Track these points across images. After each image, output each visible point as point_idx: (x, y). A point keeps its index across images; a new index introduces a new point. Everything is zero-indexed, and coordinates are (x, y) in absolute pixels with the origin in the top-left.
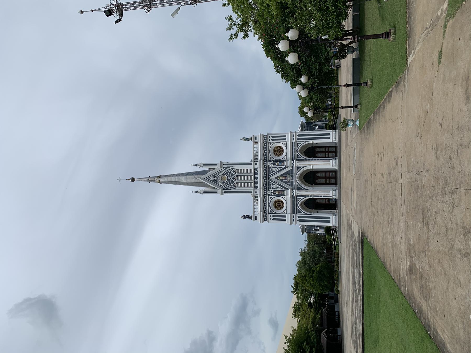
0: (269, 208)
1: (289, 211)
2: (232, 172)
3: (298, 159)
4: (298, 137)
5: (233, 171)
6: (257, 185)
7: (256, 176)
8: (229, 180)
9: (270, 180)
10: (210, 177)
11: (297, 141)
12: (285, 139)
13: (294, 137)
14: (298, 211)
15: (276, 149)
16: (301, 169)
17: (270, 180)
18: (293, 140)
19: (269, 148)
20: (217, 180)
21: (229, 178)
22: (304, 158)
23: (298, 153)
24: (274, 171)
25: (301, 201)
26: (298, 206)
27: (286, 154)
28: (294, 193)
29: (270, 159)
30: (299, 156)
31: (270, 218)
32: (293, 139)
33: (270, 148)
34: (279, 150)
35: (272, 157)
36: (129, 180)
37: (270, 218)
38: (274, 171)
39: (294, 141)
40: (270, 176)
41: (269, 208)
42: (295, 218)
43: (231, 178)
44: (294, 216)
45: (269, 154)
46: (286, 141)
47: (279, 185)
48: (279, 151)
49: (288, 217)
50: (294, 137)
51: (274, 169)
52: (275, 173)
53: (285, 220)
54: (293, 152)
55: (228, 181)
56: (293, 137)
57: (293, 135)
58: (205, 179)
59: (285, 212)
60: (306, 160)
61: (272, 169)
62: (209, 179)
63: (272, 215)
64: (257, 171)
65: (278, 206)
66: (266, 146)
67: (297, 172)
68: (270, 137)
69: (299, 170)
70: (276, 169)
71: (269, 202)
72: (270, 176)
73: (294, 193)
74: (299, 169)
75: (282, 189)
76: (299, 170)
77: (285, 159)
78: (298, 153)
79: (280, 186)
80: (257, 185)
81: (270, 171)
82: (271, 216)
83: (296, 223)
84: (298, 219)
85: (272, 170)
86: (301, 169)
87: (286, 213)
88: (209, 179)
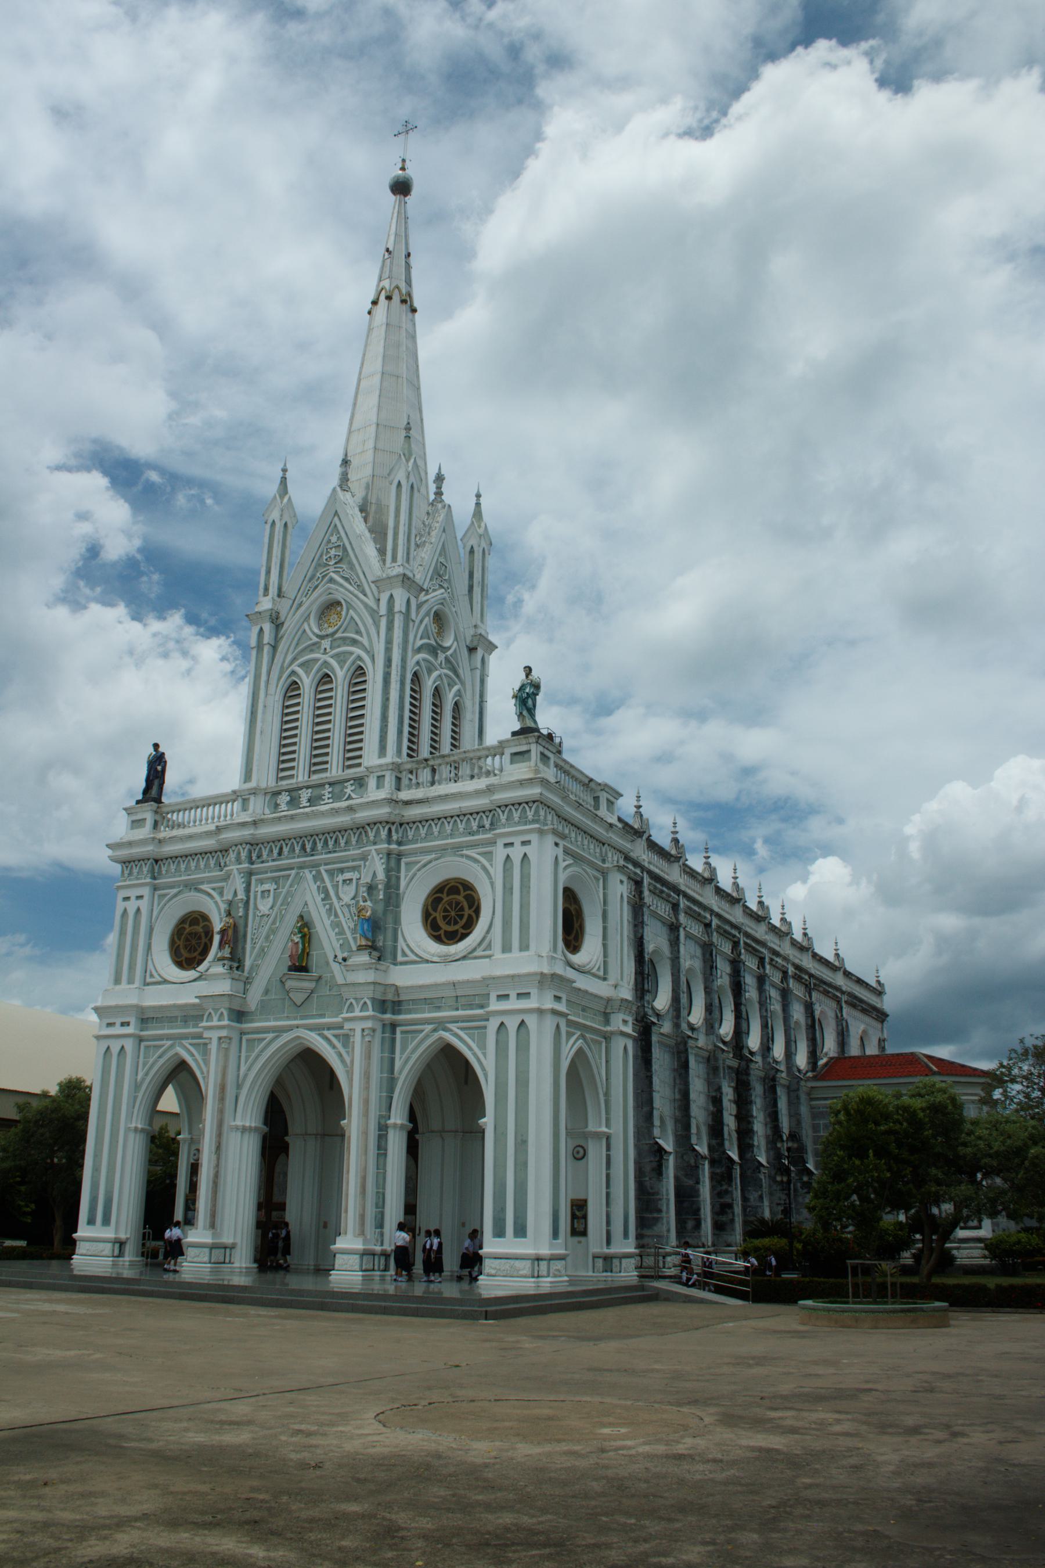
0: (175, 891)
1: (156, 998)
2: (357, 651)
3: (398, 1036)
4: (512, 1024)
5: (359, 658)
6: (283, 807)
7: (327, 795)
8: (313, 647)
9: (299, 879)
10: (339, 538)
11: (493, 1025)
12: (506, 948)
13: (513, 1004)
14: (155, 1046)
15: (463, 894)
16: (340, 1055)
17: (298, 873)
18: (500, 997)
19: (464, 852)
20: (324, 577)
21: (326, 643)
22: (400, 1073)
23: (427, 1036)
24: (339, 899)
25: (196, 1061)
26: (172, 1046)
27: (427, 961)
28: (215, 1018)
29: (407, 864)
30: (413, 1039)
31: (133, 898)
32: (506, 997)
33: (468, 857)
34: (461, 917)
35: (415, 875)
36: (403, 169)
37: (133, 898)
38: (339, 899)
39: (494, 1006)
40: (318, 877)
41: (175, 891)
42: (118, 1030)
43: (325, 652)
44: (128, 1024)
45: (428, 858)
46: (498, 955)
47: (273, 931)
48: (453, 913)
49: (129, 995)
50: (513, 1004)
51: (347, 894)
52: (331, 905)
53: (117, 981)
54: (434, 1004)
55: (315, 639)
56: (513, 995)
57: (527, 995)
58: (336, 513)
59: (152, 976)
60: (391, 1083)
61: (351, 880)
62: (334, 539)
63: (144, 905)
64: (349, 798)
65: (187, 940)
66: (477, 832)
67: (326, 1032)
68: (526, 849)
69: (334, 1047)
70: (348, 906)
71: (202, 883)
72: (319, 872)
73: (215, 1018)
74: (339, 1045)
75: (253, 948)
76: (334, 1047)
77: (404, 954)
78: (427, 1036)
79: (267, 937)
80: (283, 807)
81: (342, 871)
82: (140, 902)
83: (98, 1038)
84: (115, 1049)
85: (344, 881)
86: (340, 1055)
87: (149, 980)
88: (334, 539)
